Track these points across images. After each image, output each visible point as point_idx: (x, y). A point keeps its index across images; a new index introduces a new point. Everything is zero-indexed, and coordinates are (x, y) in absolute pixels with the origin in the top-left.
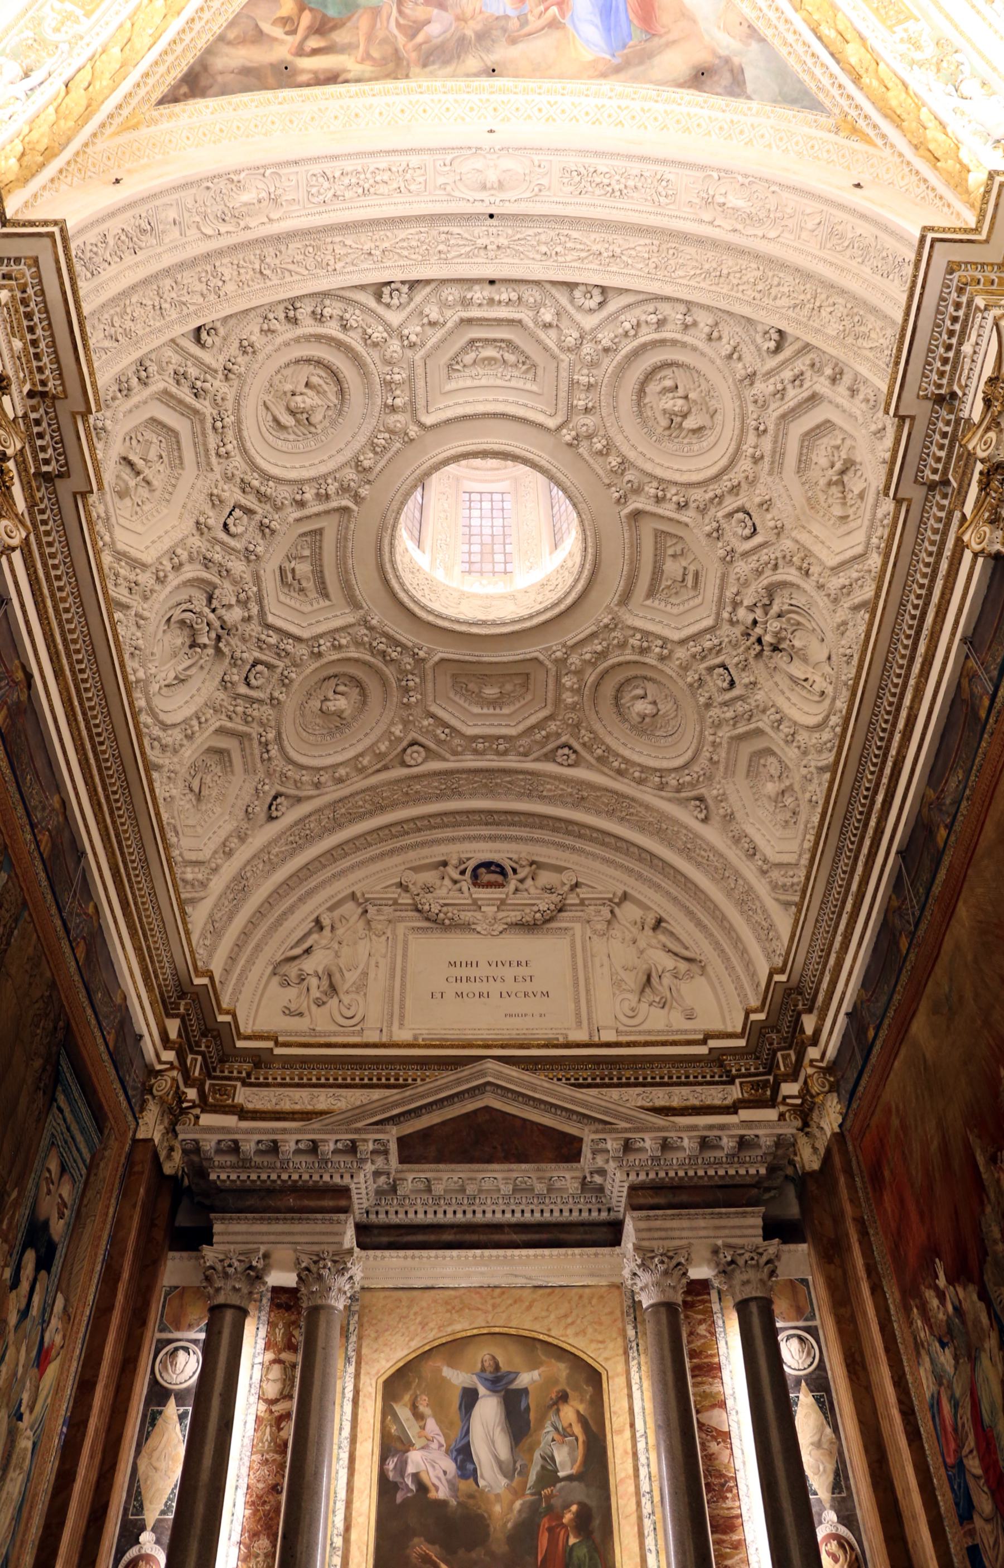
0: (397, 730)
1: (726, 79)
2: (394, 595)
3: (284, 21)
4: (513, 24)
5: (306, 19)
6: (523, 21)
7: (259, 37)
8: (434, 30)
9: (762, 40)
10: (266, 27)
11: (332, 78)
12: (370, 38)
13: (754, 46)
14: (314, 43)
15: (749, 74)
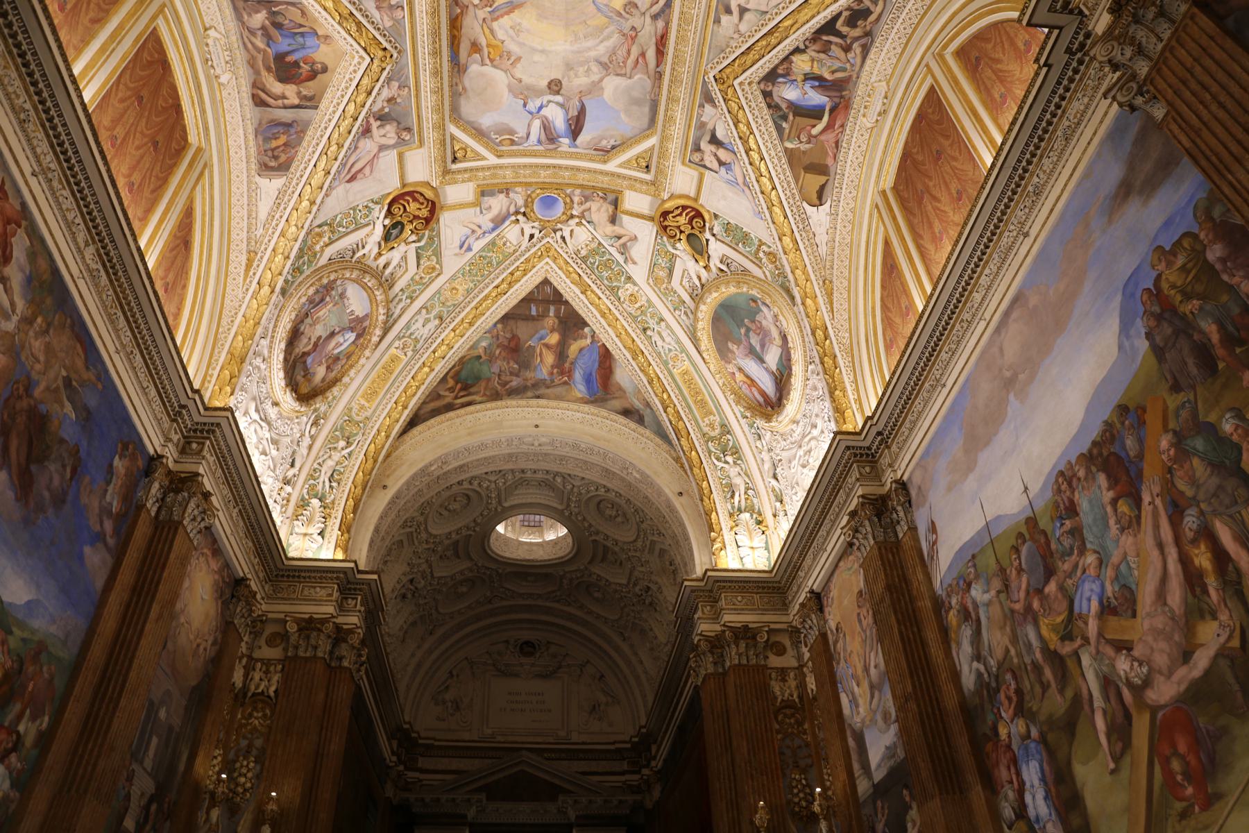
0: (488, 594)
1: (637, 417)
2: (488, 555)
3: (449, 389)
4: (548, 382)
5: (459, 386)
6: (552, 381)
7: (439, 397)
8: (514, 384)
9: (651, 409)
10: (442, 393)
11: (469, 404)
12: (485, 389)
13: (648, 410)
14: (461, 394)
15: (646, 419)
